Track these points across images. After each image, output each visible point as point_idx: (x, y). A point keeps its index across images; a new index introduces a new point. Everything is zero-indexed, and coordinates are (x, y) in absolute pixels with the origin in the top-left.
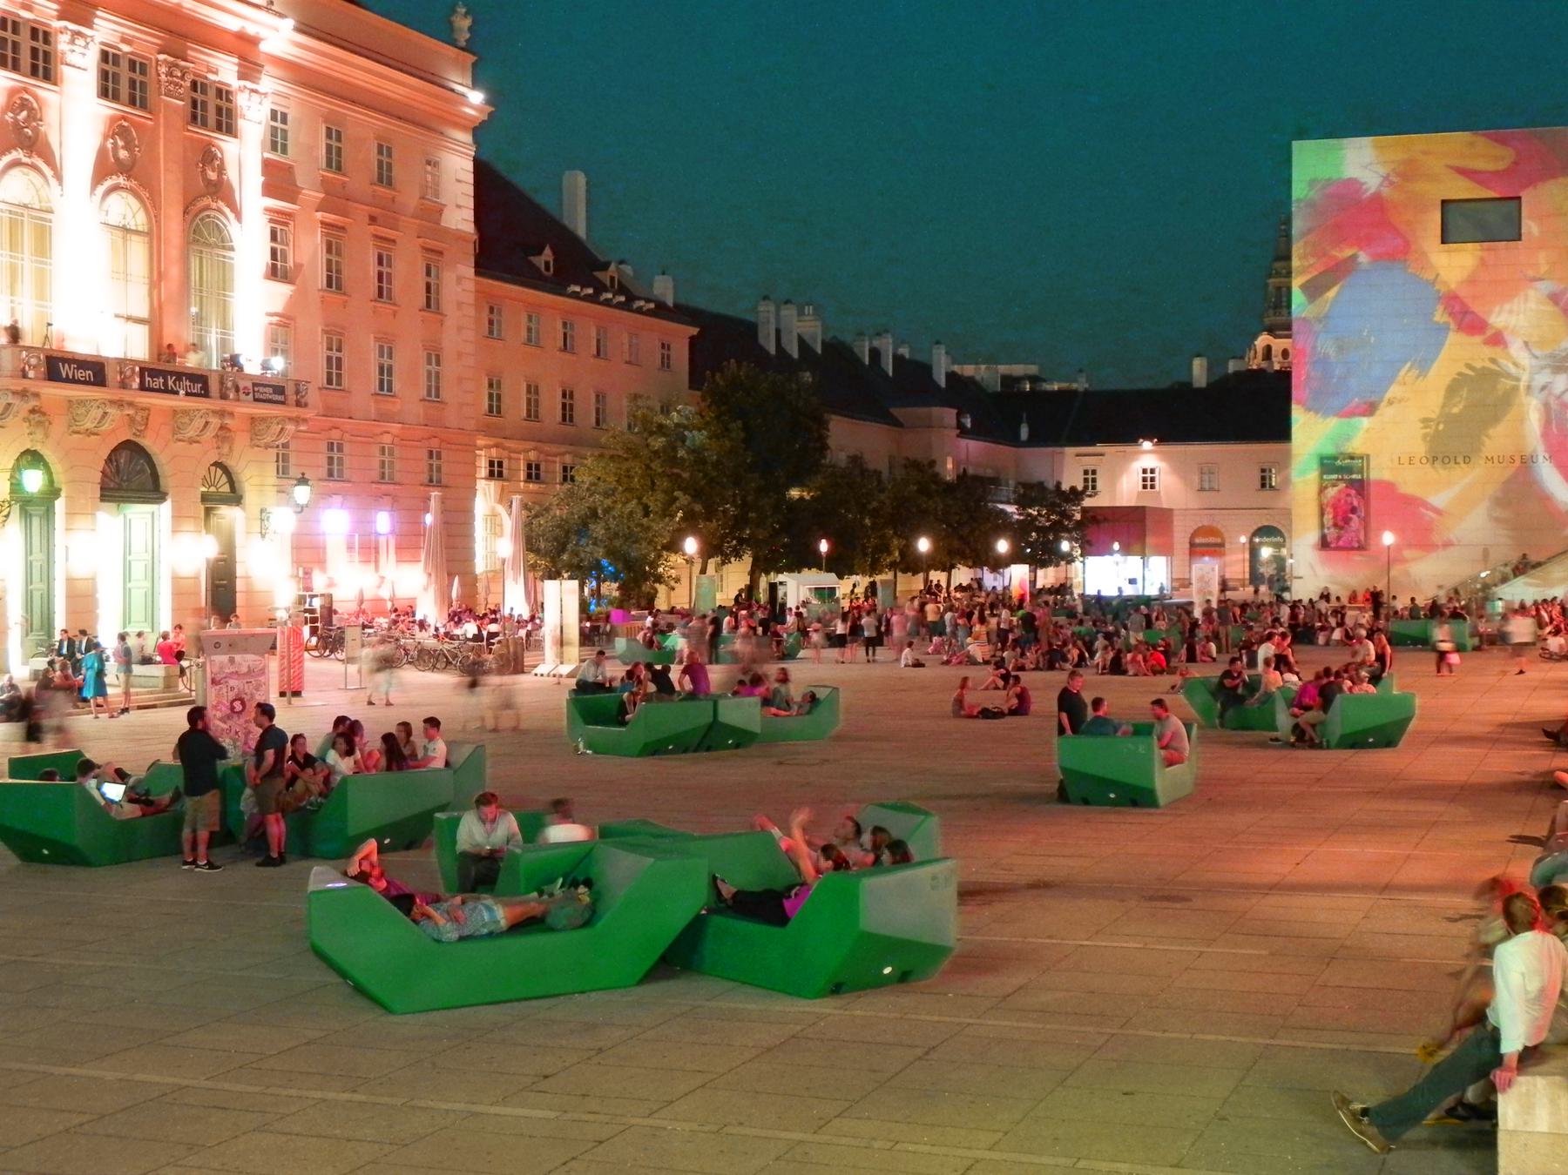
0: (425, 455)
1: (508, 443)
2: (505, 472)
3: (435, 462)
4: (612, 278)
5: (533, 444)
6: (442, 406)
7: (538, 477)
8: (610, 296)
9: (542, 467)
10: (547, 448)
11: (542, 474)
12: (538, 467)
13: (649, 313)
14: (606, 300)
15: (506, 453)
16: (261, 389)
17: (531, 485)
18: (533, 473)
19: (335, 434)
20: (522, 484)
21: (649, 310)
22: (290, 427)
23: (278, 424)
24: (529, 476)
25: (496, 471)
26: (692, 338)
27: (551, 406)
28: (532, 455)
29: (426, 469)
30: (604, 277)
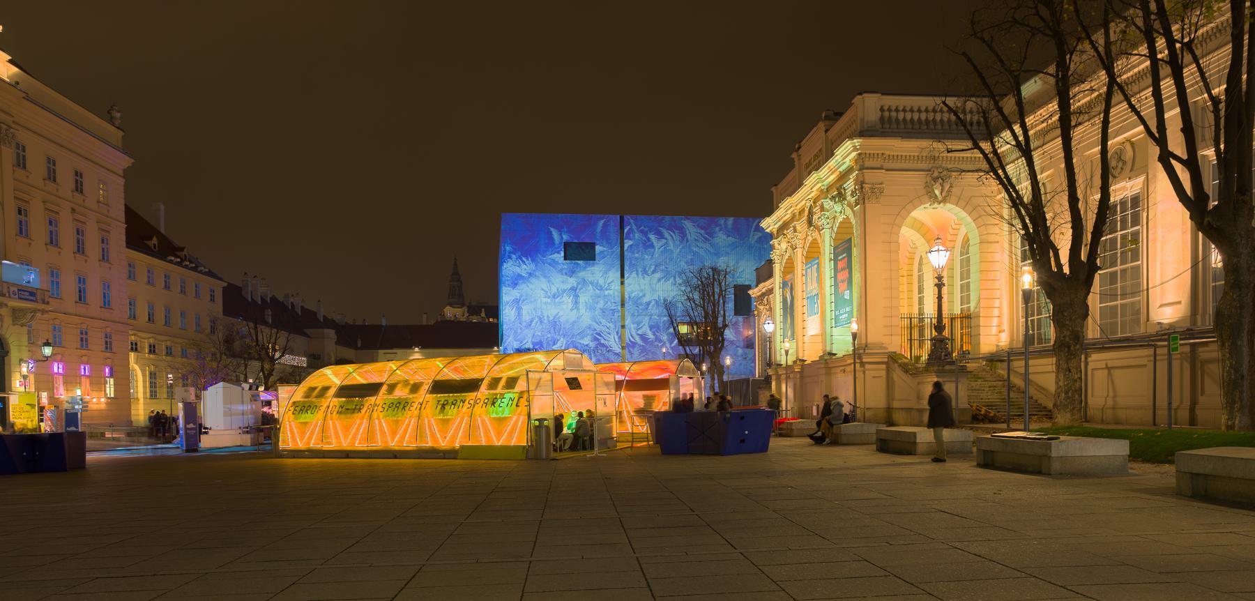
0: (104, 336)
1: (140, 334)
2: (139, 348)
3: (84, 336)
4: (185, 255)
5: (152, 335)
6: (61, 301)
7: (154, 351)
8: (188, 263)
9: (139, 345)
10: (158, 337)
11: (156, 351)
12: (154, 347)
13: (205, 274)
14: (186, 265)
15: (139, 339)
16: (23, 293)
17: (151, 356)
18: (152, 350)
19: (57, 322)
20: (147, 355)
21: (205, 272)
22: (39, 315)
23: (31, 313)
24: (150, 351)
25: (134, 348)
26: (224, 288)
27: (160, 317)
28: (152, 341)
29: (104, 343)
30: (182, 254)
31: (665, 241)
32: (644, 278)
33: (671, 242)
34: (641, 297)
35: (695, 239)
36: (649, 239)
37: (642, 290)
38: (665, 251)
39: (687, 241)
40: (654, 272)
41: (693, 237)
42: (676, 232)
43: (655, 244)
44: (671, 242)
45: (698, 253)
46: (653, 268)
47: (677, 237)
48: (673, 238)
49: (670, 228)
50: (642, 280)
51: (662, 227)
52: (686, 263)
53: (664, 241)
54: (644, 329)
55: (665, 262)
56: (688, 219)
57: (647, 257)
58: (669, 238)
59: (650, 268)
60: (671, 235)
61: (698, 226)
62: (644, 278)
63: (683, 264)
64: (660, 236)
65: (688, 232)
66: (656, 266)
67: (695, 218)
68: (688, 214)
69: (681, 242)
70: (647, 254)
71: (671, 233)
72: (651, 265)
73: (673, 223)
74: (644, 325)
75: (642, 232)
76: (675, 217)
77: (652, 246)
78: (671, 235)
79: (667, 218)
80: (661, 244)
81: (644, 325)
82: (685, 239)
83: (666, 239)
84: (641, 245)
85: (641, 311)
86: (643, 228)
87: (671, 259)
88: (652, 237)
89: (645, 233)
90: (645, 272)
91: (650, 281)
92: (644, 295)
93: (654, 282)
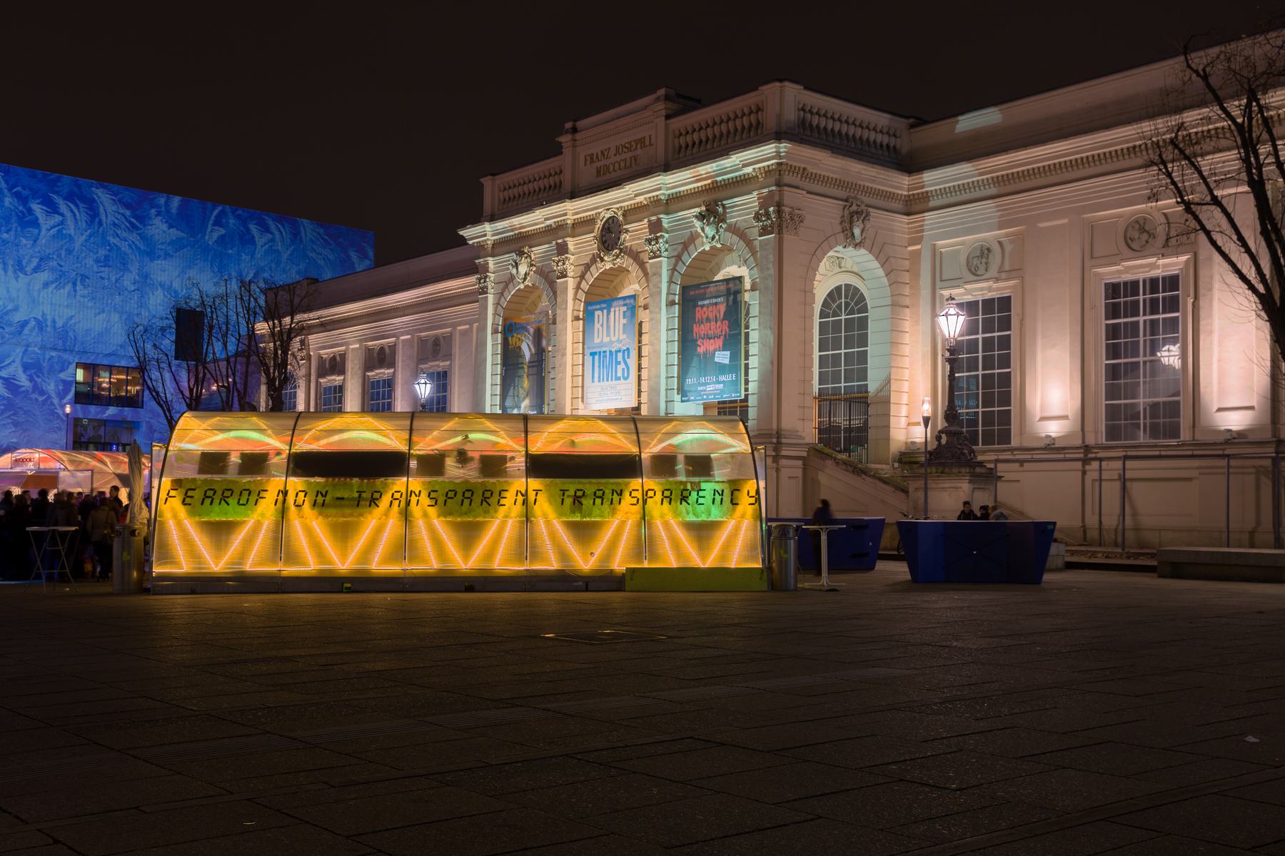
31: (61, 218)
32: (17, 278)
33: (70, 222)
34: (10, 311)
35: (115, 224)
36: (30, 211)
37: (12, 300)
38: (59, 235)
39: (100, 224)
40: (36, 270)
41: (111, 218)
42: (81, 205)
43: (41, 221)
44: (70, 222)
45: (119, 249)
46: (35, 262)
47: (82, 216)
48: (75, 215)
49: (70, 197)
50: (13, 281)
51: (57, 193)
52: (97, 261)
53: (58, 218)
54: (11, 369)
55: (59, 256)
56: (105, 187)
57: (24, 241)
58: (68, 214)
59: (30, 261)
60: (72, 211)
61: (120, 201)
62: (17, 278)
63: (90, 262)
64: (53, 209)
65: (101, 209)
66: (41, 259)
67: (115, 188)
68: (105, 177)
69: (90, 223)
70: (24, 237)
71: (72, 206)
72: (32, 257)
73: (76, 189)
74: (14, 361)
75: (17, 195)
76: (82, 181)
77: (35, 223)
78: (72, 211)
79: (67, 179)
80: (52, 222)
81: (14, 361)
82: (97, 220)
83: (62, 215)
84: (14, 219)
85: (7, 336)
86: (19, 188)
87: (69, 252)
88: (37, 208)
89: (24, 200)
90: (20, 267)
91: (29, 284)
92: (16, 309)
93: (37, 288)
